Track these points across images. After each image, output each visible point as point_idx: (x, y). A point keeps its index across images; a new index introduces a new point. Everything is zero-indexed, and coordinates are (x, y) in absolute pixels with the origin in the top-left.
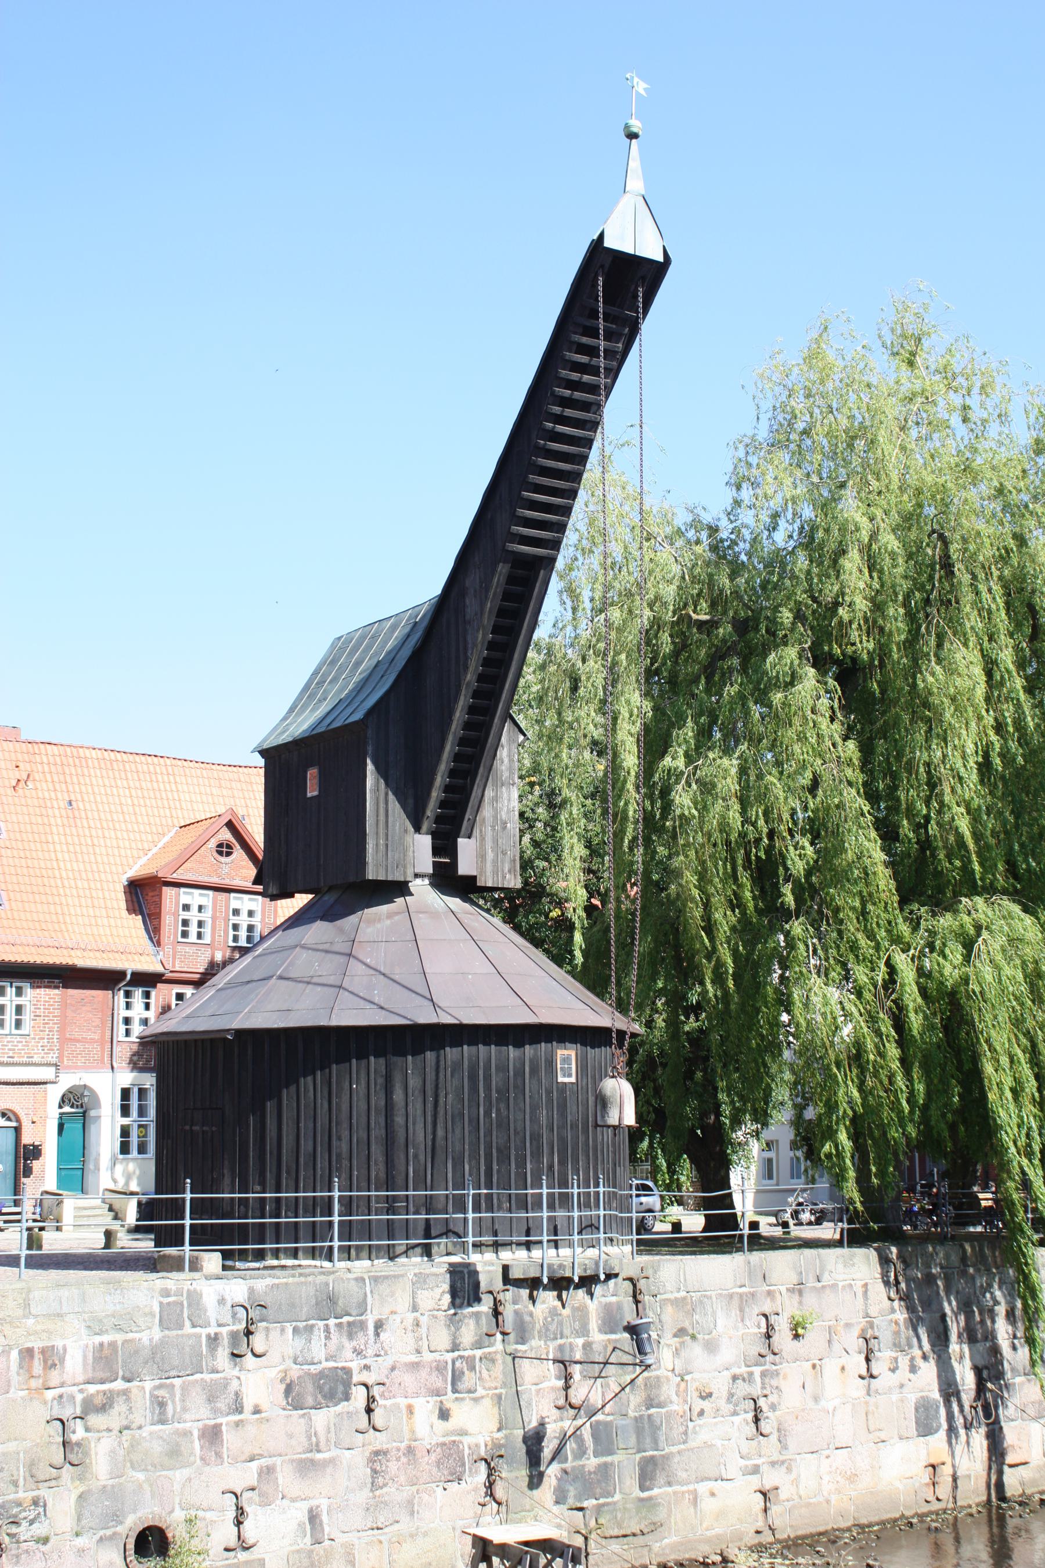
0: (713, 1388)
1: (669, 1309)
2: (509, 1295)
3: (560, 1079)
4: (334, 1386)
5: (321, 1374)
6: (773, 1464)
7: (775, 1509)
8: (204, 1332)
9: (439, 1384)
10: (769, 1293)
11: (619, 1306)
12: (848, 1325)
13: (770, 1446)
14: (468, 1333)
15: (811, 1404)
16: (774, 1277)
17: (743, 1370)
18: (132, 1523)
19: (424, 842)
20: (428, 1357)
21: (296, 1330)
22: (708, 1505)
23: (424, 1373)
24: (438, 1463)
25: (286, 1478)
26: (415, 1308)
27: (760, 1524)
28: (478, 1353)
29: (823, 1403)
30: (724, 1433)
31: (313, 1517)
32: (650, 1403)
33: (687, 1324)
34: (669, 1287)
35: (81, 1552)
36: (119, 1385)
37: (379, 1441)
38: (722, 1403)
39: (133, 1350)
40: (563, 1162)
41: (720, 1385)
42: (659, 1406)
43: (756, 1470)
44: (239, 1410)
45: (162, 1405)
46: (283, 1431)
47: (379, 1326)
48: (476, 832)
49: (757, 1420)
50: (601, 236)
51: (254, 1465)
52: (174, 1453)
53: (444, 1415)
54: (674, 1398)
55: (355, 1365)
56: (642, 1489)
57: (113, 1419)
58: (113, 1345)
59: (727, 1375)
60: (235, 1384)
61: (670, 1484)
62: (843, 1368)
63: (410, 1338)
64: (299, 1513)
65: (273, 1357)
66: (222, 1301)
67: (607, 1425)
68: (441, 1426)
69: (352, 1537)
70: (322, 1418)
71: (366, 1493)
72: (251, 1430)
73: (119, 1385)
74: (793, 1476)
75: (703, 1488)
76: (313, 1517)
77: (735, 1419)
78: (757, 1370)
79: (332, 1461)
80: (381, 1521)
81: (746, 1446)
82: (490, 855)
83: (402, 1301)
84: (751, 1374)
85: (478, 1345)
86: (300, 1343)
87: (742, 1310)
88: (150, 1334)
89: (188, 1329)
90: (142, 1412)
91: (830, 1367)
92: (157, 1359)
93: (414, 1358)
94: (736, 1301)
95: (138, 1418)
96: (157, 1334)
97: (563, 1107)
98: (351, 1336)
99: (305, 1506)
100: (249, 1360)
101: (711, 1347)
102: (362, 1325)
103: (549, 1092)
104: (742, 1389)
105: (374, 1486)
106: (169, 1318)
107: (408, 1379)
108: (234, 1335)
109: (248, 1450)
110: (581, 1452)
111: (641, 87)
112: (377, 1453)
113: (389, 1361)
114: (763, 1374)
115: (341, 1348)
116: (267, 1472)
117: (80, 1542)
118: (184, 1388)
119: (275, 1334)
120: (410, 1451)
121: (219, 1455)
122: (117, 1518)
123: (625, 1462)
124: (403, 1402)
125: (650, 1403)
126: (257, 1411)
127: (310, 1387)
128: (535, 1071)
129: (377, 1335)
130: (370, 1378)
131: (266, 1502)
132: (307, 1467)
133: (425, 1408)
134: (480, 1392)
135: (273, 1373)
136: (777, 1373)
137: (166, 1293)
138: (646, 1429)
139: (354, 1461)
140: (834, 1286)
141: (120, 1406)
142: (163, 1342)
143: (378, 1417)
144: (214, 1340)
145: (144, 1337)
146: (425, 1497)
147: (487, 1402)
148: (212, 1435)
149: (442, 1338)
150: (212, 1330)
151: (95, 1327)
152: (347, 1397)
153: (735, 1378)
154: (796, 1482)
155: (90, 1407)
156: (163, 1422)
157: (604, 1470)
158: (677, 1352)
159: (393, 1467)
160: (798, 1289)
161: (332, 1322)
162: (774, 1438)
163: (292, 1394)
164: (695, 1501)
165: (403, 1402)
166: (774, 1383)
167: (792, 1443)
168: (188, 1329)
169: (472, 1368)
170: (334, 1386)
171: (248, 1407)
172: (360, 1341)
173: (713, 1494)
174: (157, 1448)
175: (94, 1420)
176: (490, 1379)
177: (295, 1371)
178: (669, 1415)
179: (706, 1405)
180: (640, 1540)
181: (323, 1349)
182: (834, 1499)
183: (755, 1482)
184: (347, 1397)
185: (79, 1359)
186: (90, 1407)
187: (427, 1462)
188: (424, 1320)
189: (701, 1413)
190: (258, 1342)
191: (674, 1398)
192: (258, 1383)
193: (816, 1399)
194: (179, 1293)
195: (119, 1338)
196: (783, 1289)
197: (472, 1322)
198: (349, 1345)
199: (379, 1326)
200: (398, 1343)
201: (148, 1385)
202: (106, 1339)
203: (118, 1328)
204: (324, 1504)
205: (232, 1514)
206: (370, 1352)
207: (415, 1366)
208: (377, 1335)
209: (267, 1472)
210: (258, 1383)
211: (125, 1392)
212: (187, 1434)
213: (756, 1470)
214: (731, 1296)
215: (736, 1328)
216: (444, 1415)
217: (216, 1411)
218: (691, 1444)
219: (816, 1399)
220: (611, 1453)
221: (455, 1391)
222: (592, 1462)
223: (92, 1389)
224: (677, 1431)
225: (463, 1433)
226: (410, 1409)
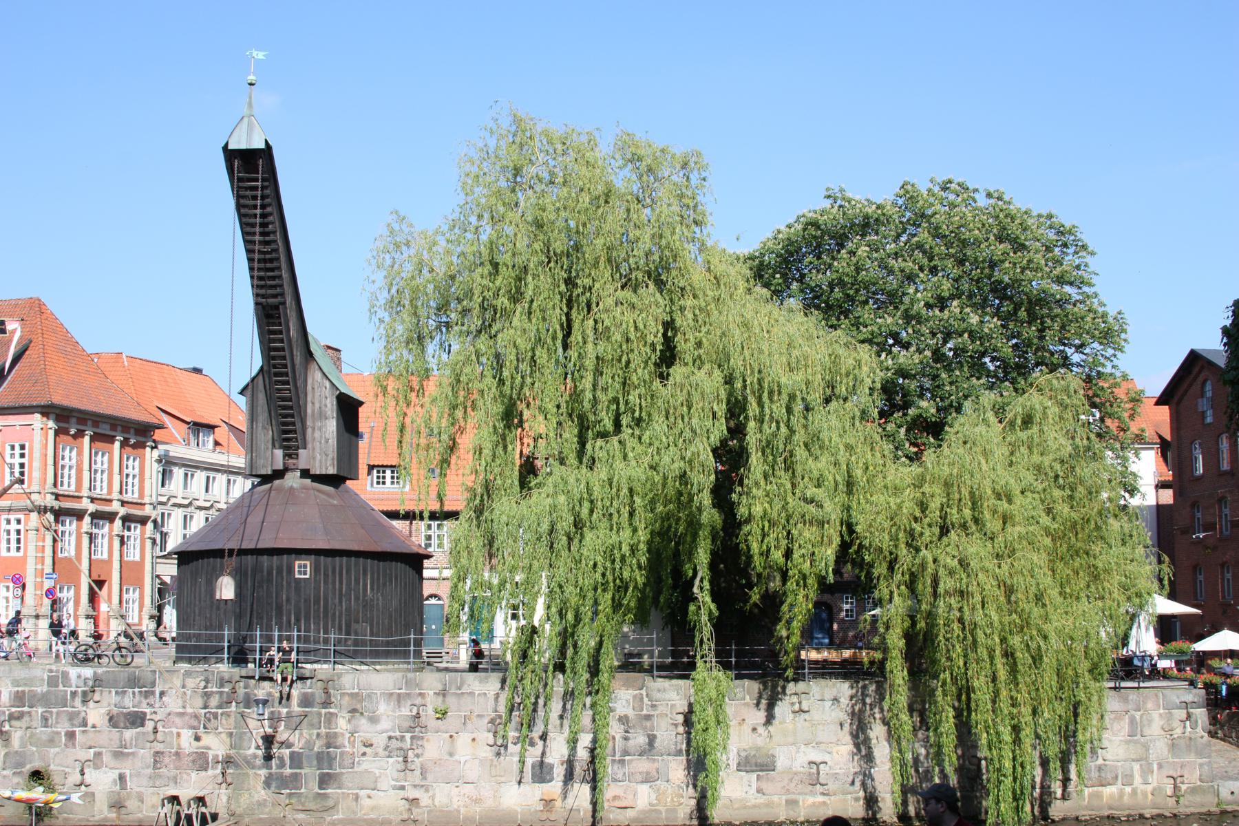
0: (374, 741)
1: (347, 698)
2: (242, 684)
3: (297, 576)
4: (137, 720)
5: (129, 713)
6: (415, 786)
7: (416, 811)
8: (69, 690)
9: (196, 724)
10: (420, 694)
11: (313, 694)
12: (479, 716)
13: (416, 777)
14: (214, 701)
15: (447, 757)
16: (425, 685)
17: (398, 734)
18: (29, 768)
19: (279, 453)
20: (189, 710)
21: (117, 693)
22: (366, 802)
23: (187, 718)
24: (193, 761)
25: (107, 758)
26: (184, 687)
27: (405, 816)
28: (220, 711)
29: (456, 757)
30: (385, 769)
31: (122, 778)
32: (329, 746)
33: (358, 707)
34: (347, 686)
35: (4, 777)
36: (26, 709)
37: (159, 747)
38: (381, 751)
39: (33, 695)
40: (298, 620)
41: (380, 741)
42: (335, 747)
43: (403, 788)
44: (85, 724)
45: (46, 720)
46: (108, 737)
47: (162, 694)
48: (310, 446)
49: (406, 761)
50: (227, 144)
51: (92, 751)
52: (51, 742)
53: (197, 739)
54: (347, 744)
55: (148, 711)
56: (320, 788)
57: (25, 722)
58: (23, 692)
59: (385, 735)
60: (83, 714)
61: (340, 788)
62: (474, 739)
63: (180, 701)
64: (114, 774)
65: (104, 703)
66: (79, 677)
67: (299, 753)
68: (195, 744)
69: (142, 789)
70: (129, 734)
71: (150, 771)
72: (91, 735)
73: (26, 709)
74: (431, 793)
75: (363, 793)
76: (122, 778)
77: (390, 760)
78: (408, 736)
79: (132, 753)
80: (157, 783)
81: (396, 775)
82: (318, 457)
83: (178, 682)
84: (403, 737)
85: (220, 707)
86: (119, 698)
87: (399, 702)
88: (42, 689)
89: (61, 687)
90: (37, 722)
91: (463, 740)
92: (45, 700)
93: (181, 710)
94: (395, 697)
95: (34, 724)
96: (45, 689)
97: (298, 589)
98: (146, 697)
99: (117, 772)
100: (91, 704)
101: (374, 720)
102: (153, 693)
103: (289, 583)
104: (395, 744)
105: (155, 768)
106: (52, 682)
107: (178, 720)
108: (84, 693)
109: (89, 743)
110: (282, 765)
111: (260, 55)
112: (157, 752)
113: (168, 710)
114: (412, 738)
115: (140, 702)
116: (98, 755)
117: (5, 773)
118: (58, 713)
119: (105, 694)
120: (177, 754)
121: (74, 745)
122: (20, 765)
123: (310, 773)
124: (175, 730)
125: (329, 746)
126: (94, 727)
127: (122, 719)
128: (280, 571)
129: (161, 697)
130: (157, 718)
131: (97, 767)
132: (118, 755)
133: (187, 735)
134: (220, 729)
135: (103, 711)
136: (422, 738)
137: (51, 671)
138: (324, 759)
139: (146, 754)
140: (472, 694)
141: (26, 718)
142: (48, 692)
143: (160, 736)
144: (74, 694)
145: (39, 690)
146: (185, 776)
147: (224, 736)
148: (71, 735)
149: (199, 702)
150: (73, 689)
151: (16, 683)
152: (143, 725)
153: (390, 738)
154: (433, 798)
155: (12, 717)
156: (46, 726)
157: (296, 777)
158: (349, 721)
159: (167, 760)
160: (443, 693)
161: (137, 690)
162: (418, 772)
163: (112, 721)
164: (357, 798)
165: (175, 730)
166: (420, 743)
167: (430, 777)
168: (61, 687)
169: (216, 717)
170: (137, 720)
171: (90, 724)
172: (151, 700)
173: (369, 797)
174: (44, 737)
175: (14, 723)
176: (225, 725)
177: (115, 711)
178: (342, 754)
179: (368, 750)
180: (319, 814)
181: (130, 702)
182: (463, 810)
183: (402, 793)
184: (143, 725)
185: (7, 695)
186: (12, 717)
187: (186, 760)
188: (189, 693)
189: (364, 754)
190: (97, 697)
191: (347, 744)
192: (96, 715)
193: (451, 754)
194: (57, 671)
195: (27, 689)
196: (431, 693)
197: (217, 696)
198: (145, 702)
199: (162, 694)
200: (173, 703)
201: (40, 710)
202: (20, 689)
203: (26, 685)
204: (128, 773)
205: (78, 770)
206: (157, 705)
207: (182, 714)
208: (161, 697)
209: (98, 755)
210: (96, 715)
211: (29, 713)
212: (59, 733)
213: (403, 788)
214: (391, 694)
215: (394, 711)
216: (197, 739)
217: (73, 725)
218: (356, 769)
219: (451, 754)
220: (301, 768)
221: (205, 727)
222: (288, 771)
223: (13, 709)
224: (347, 762)
225: (209, 748)
226: (179, 735)
